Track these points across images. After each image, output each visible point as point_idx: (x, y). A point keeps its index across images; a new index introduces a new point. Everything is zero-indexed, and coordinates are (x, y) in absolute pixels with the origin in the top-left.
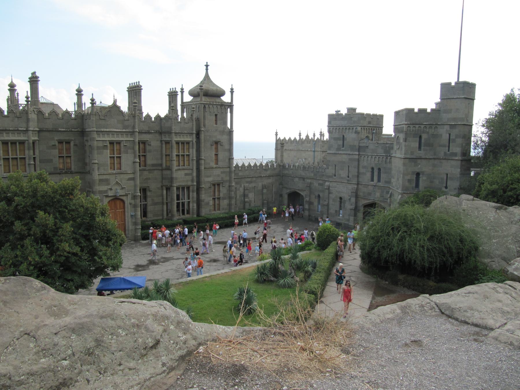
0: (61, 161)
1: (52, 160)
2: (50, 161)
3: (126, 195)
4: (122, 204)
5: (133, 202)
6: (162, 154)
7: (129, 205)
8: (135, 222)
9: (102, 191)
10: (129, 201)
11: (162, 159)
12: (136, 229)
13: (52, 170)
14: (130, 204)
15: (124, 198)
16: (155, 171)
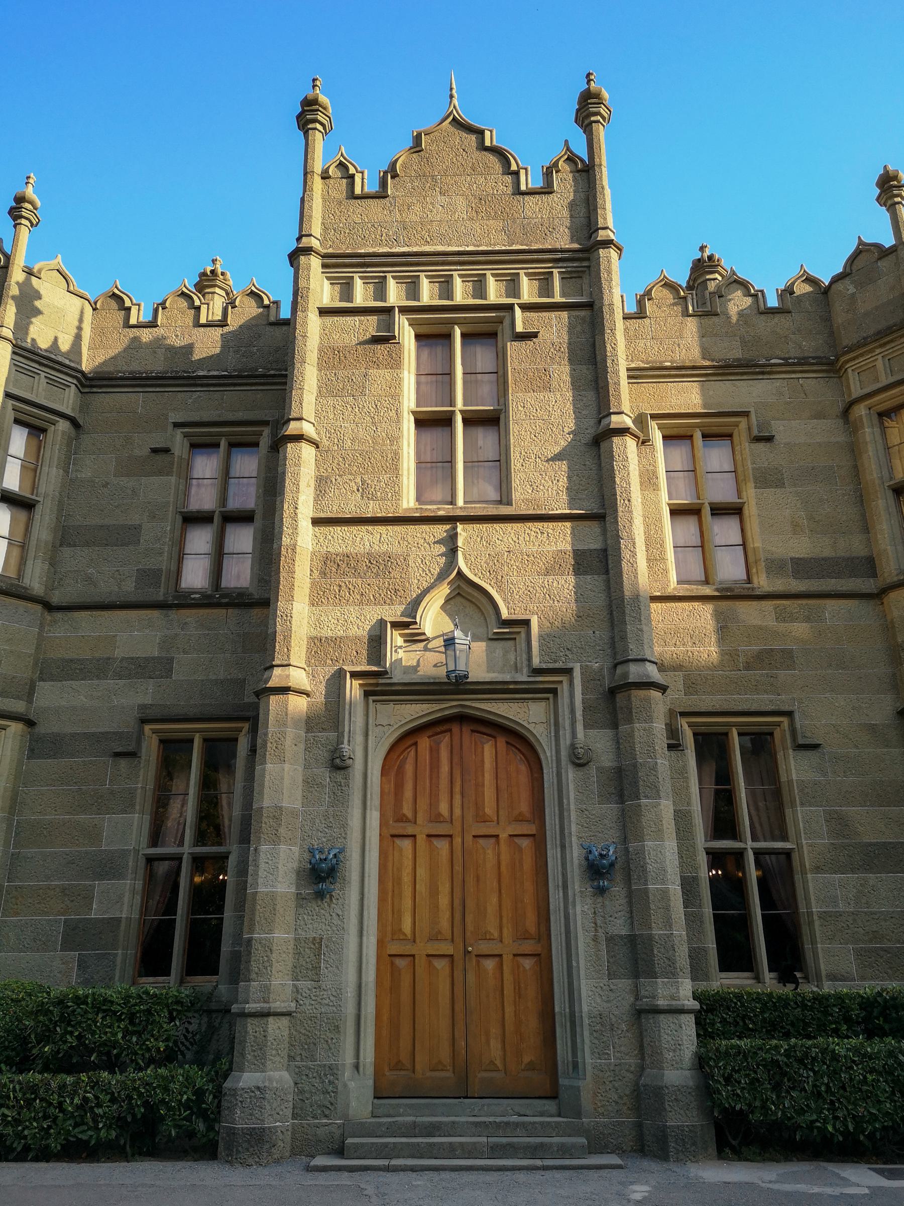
0: (200, 540)
1: (137, 529)
2: (127, 536)
3: (541, 685)
4: (521, 772)
5: (599, 743)
6: (861, 498)
7: (571, 775)
8: (632, 941)
9: (335, 641)
10: (565, 742)
11: (866, 528)
12: (644, 1013)
13: (129, 588)
14: (579, 762)
15: (530, 716)
16: (830, 604)
